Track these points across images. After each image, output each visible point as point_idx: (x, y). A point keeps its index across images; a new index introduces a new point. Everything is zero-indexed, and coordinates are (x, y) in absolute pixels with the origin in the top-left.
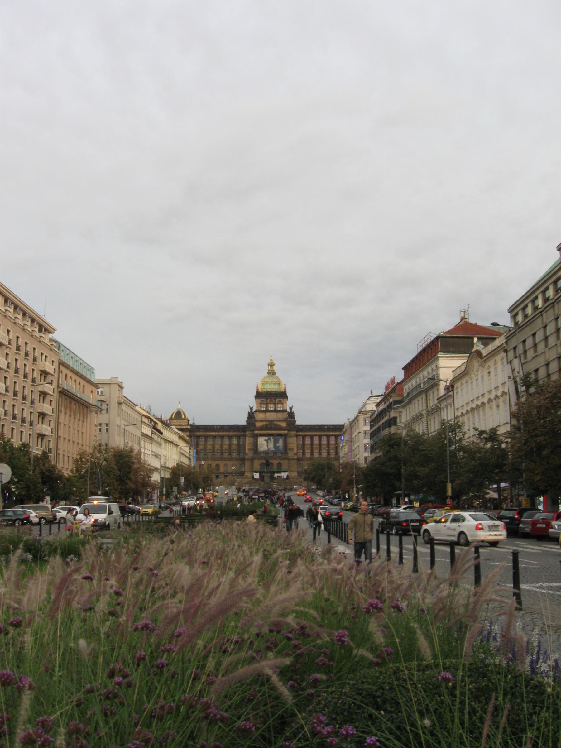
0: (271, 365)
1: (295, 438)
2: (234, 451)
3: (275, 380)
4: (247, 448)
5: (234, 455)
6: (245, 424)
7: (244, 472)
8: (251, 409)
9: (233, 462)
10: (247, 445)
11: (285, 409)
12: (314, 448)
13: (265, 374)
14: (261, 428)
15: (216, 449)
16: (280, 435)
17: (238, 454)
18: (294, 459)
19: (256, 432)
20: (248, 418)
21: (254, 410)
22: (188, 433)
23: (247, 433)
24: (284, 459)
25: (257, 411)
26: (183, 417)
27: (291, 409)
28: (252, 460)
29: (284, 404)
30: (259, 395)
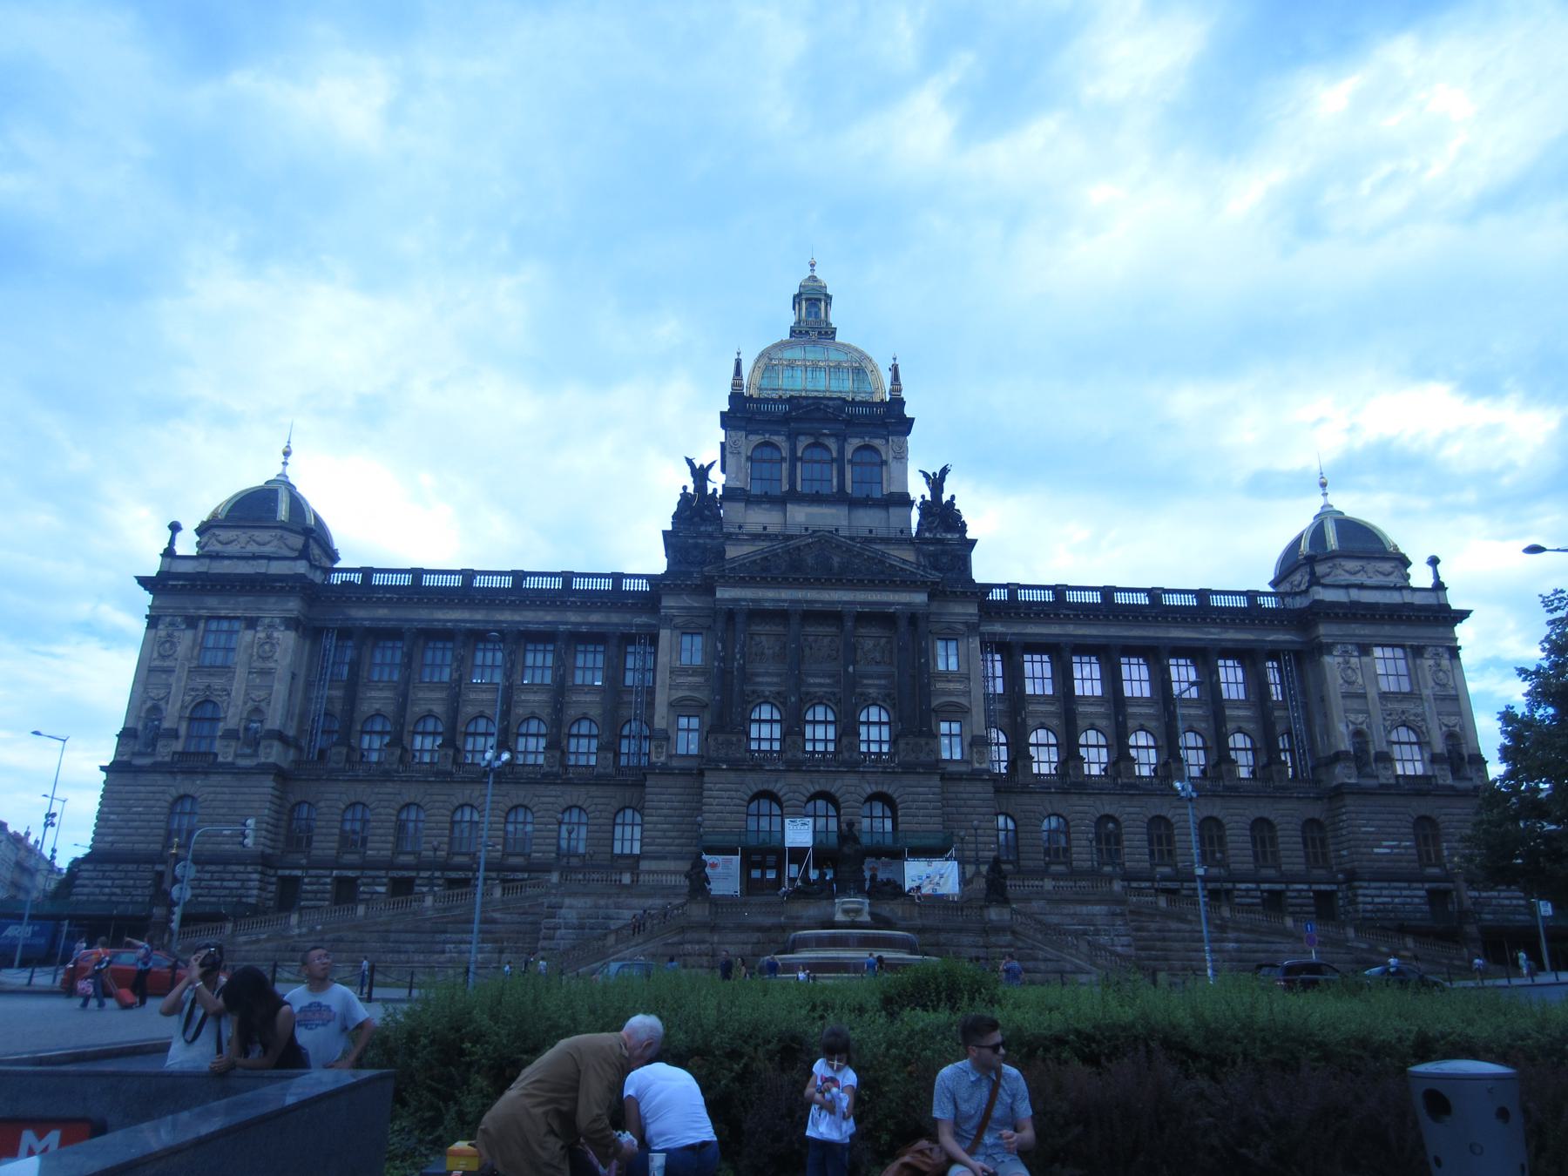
0: (812, 299)
1: (975, 643)
2: (584, 728)
3: (834, 356)
4: (661, 699)
5: (584, 751)
6: (658, 564)
7: (638, 858)
8: (700, 474)
9: (577, 795)
10: (663, 677)
11: (894, 489)
12: (1081, 723)
13: (786, 336)
14: (759, 572)
15: (470, 710)
16: (882, 618)
17: (610, 746)
18: (975, 776)
19: (722, 593)
20: (676, 517)
21: (717, 481)
22: (293, 606)
23: (668, 602)
24: (909, 769)
25: (730, 493)
26: (283, 512)
27: (936, 483)
28: (695, 772)
29: (894, 465)
30: (742, 414)
